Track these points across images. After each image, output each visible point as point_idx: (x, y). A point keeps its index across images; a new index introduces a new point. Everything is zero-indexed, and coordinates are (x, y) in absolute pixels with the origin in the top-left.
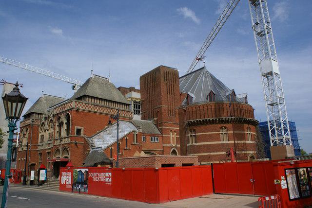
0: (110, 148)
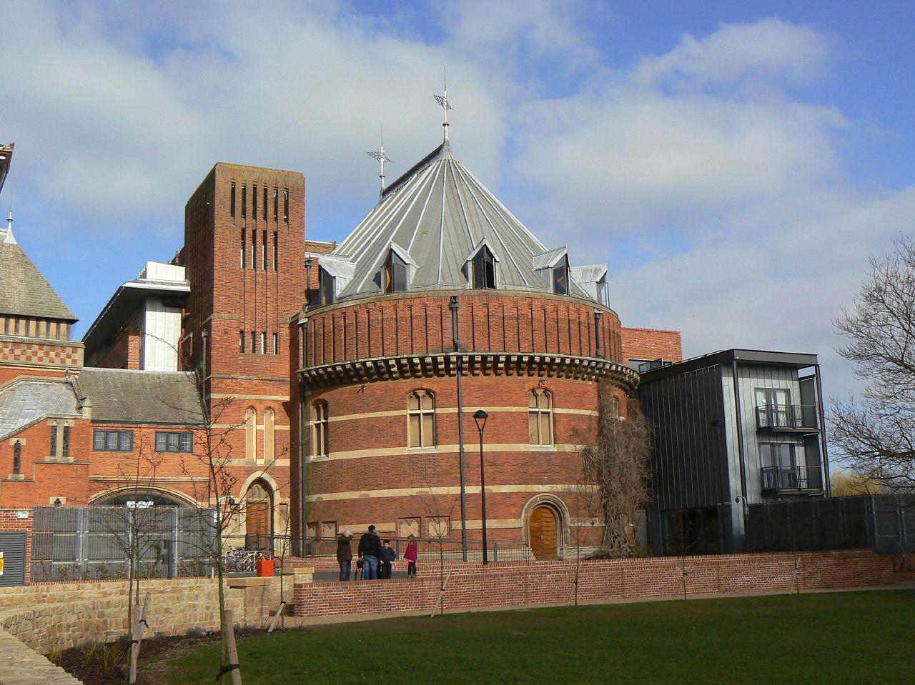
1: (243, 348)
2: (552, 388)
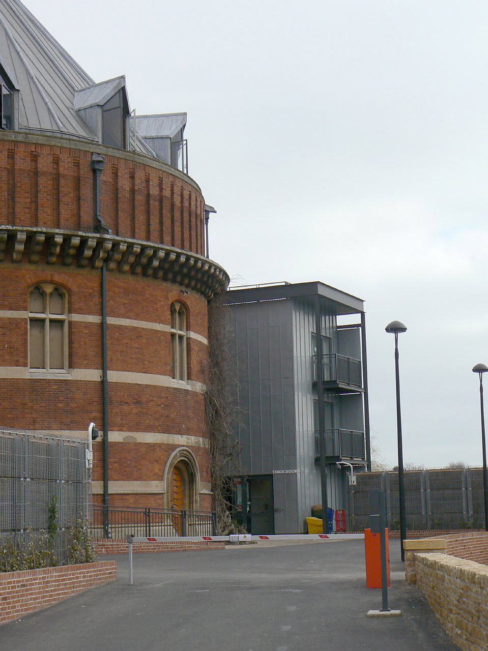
2: (189, 303)
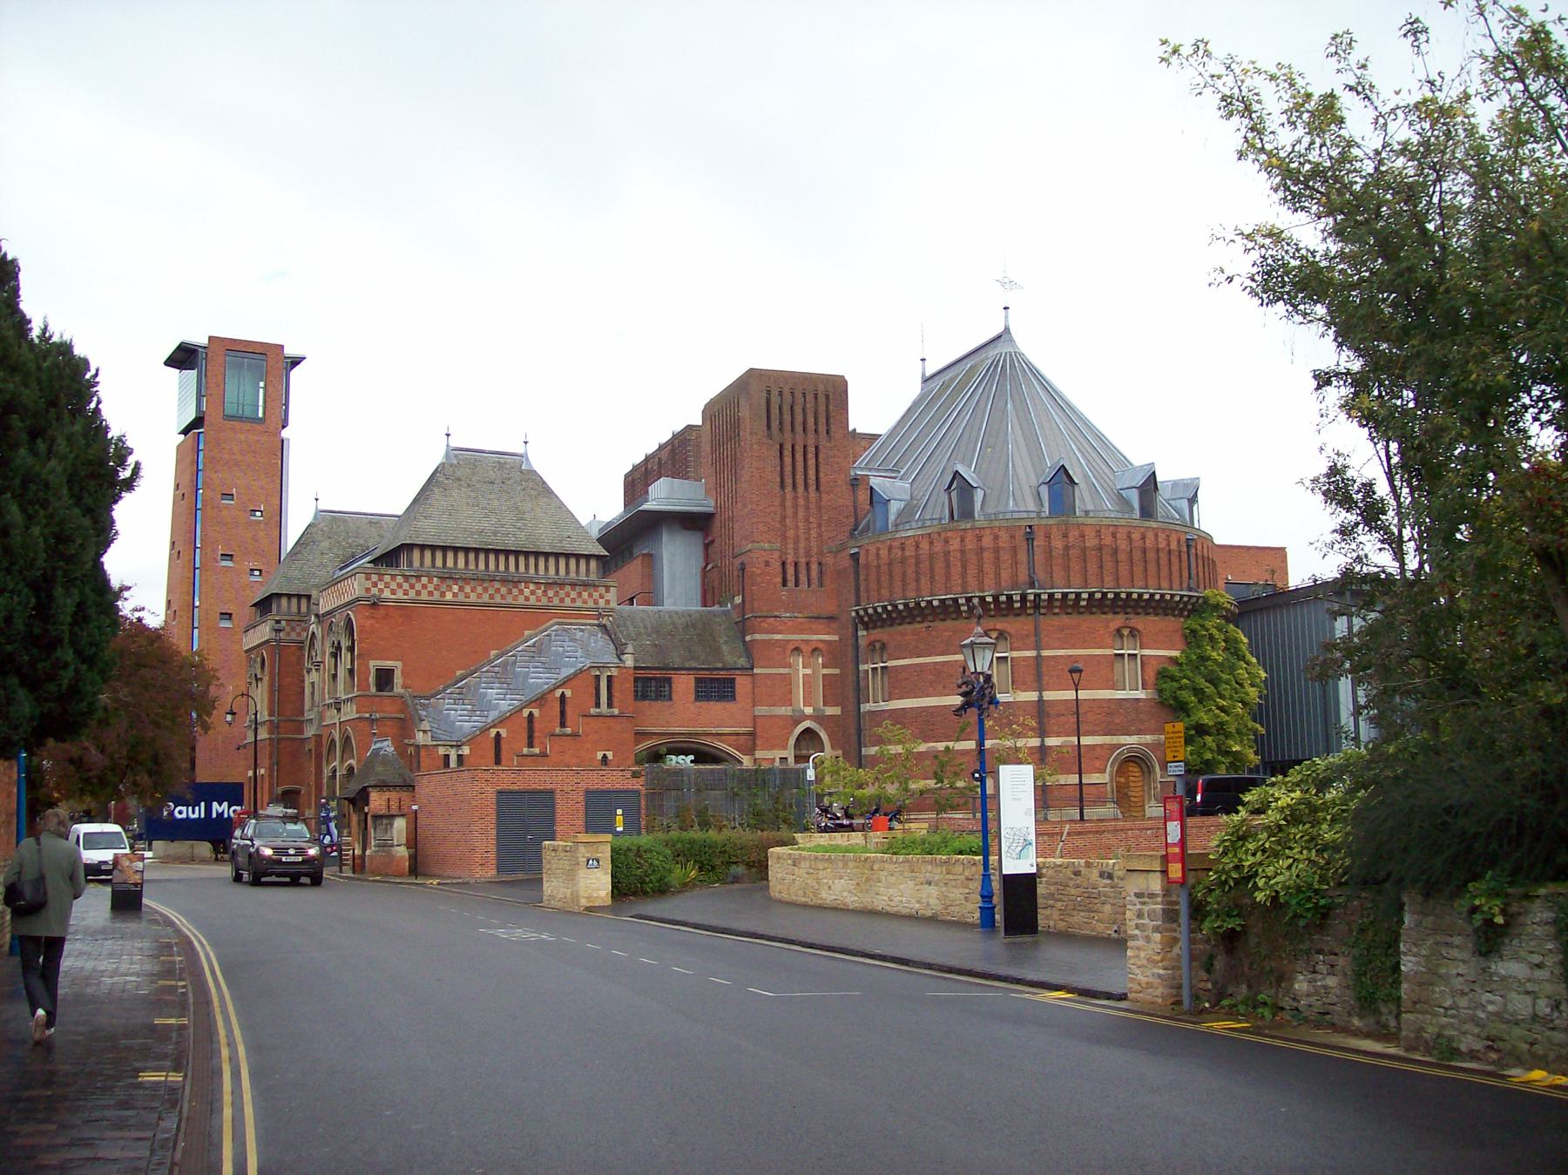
0: (493, 732)
1: (784, 583)
